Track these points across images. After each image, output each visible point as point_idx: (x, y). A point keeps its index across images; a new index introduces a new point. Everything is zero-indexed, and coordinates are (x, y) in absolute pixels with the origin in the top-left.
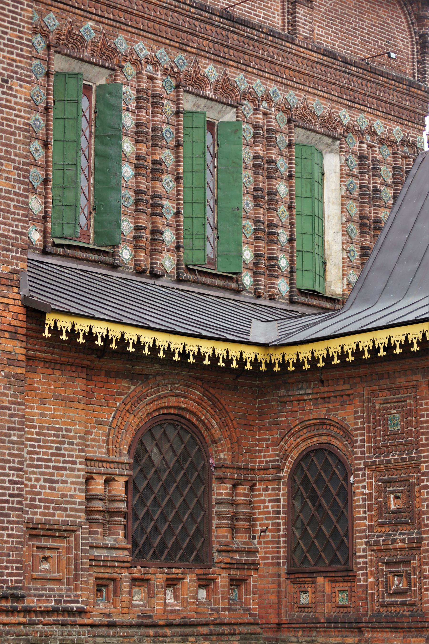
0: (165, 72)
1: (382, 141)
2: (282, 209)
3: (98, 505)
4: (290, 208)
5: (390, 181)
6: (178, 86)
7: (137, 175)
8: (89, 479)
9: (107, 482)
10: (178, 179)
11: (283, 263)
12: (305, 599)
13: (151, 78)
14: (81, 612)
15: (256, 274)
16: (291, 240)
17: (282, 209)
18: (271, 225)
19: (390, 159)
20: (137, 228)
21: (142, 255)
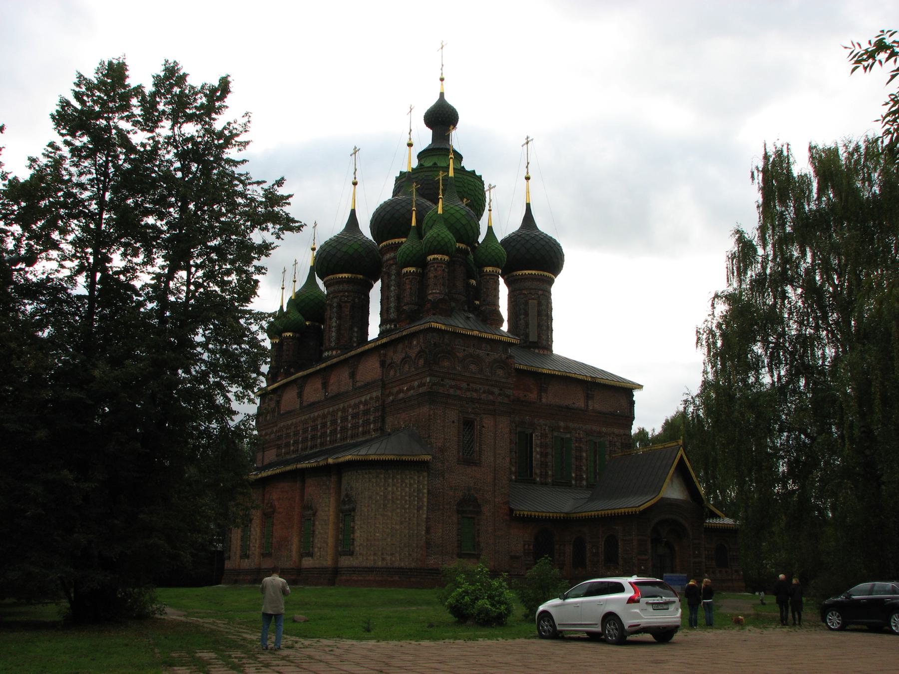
0: (549, 427)
1: (617, 435)
2: (584, 461)
3: (527, 551)
4: (587, 460)
5: (620, 447)
6: (552, 430)
7: (541, 457)
8: (524, 545)
9: (529, 545)
10: (553, 457)
11: (585, 476)
12: (576, 572)
13: (545, 429)
14: (522, 575)
15: (576, 481)
16: (587, 469)
17: (584, 461)
18: (581, 466)
19: (620, 441)
20: (541, 472)
21: (542, 479)
